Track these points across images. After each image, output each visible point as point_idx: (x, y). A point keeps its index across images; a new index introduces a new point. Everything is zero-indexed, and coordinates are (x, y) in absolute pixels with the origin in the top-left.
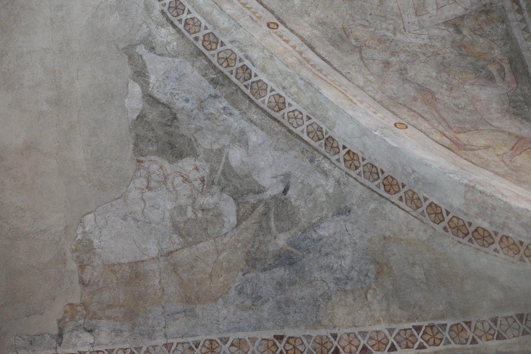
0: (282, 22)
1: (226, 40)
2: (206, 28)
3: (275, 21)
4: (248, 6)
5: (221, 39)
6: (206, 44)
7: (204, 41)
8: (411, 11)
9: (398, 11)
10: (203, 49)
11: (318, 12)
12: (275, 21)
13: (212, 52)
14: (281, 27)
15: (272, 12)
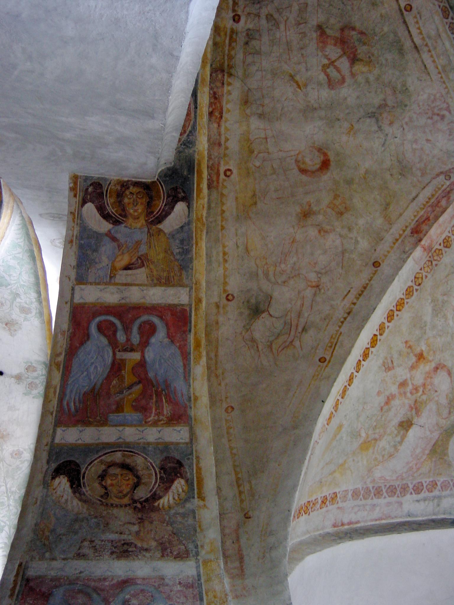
0: (401, 10)
1: (437, 7)
2: (447, 23)
3: (405, 13)
4: (418, 31)
5: (440, 10)
6: (447, 12)
7: (449, 15)
8: (309, 9)
9: (319, 10)
10: (450, 10)
11: (374, 17)
12: (405, 13)
13: (445, 5)
14: (403, 5)
15: (405, 22)
